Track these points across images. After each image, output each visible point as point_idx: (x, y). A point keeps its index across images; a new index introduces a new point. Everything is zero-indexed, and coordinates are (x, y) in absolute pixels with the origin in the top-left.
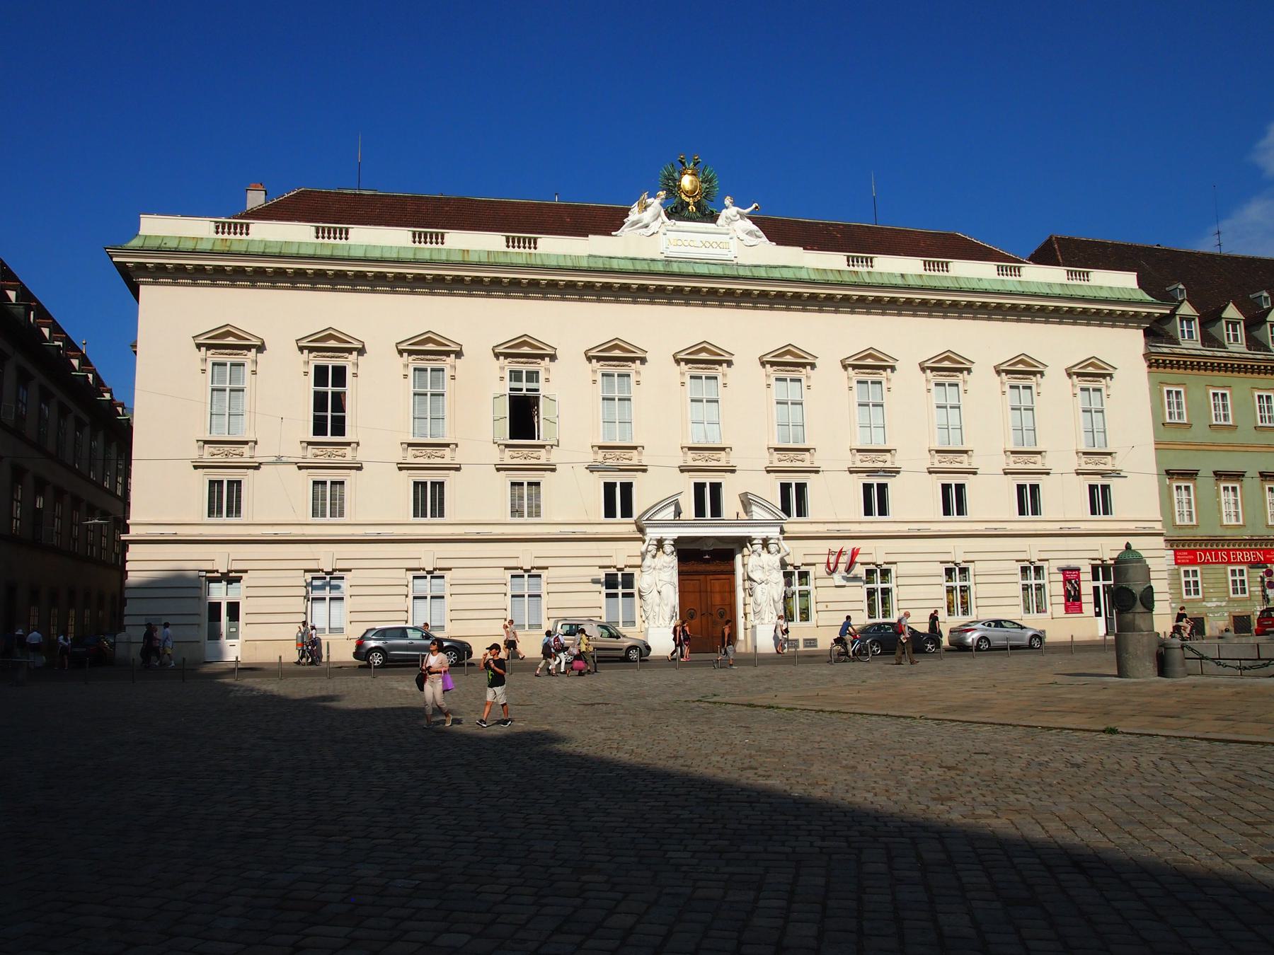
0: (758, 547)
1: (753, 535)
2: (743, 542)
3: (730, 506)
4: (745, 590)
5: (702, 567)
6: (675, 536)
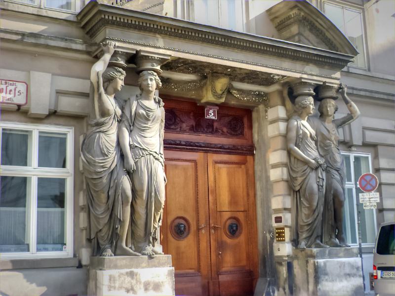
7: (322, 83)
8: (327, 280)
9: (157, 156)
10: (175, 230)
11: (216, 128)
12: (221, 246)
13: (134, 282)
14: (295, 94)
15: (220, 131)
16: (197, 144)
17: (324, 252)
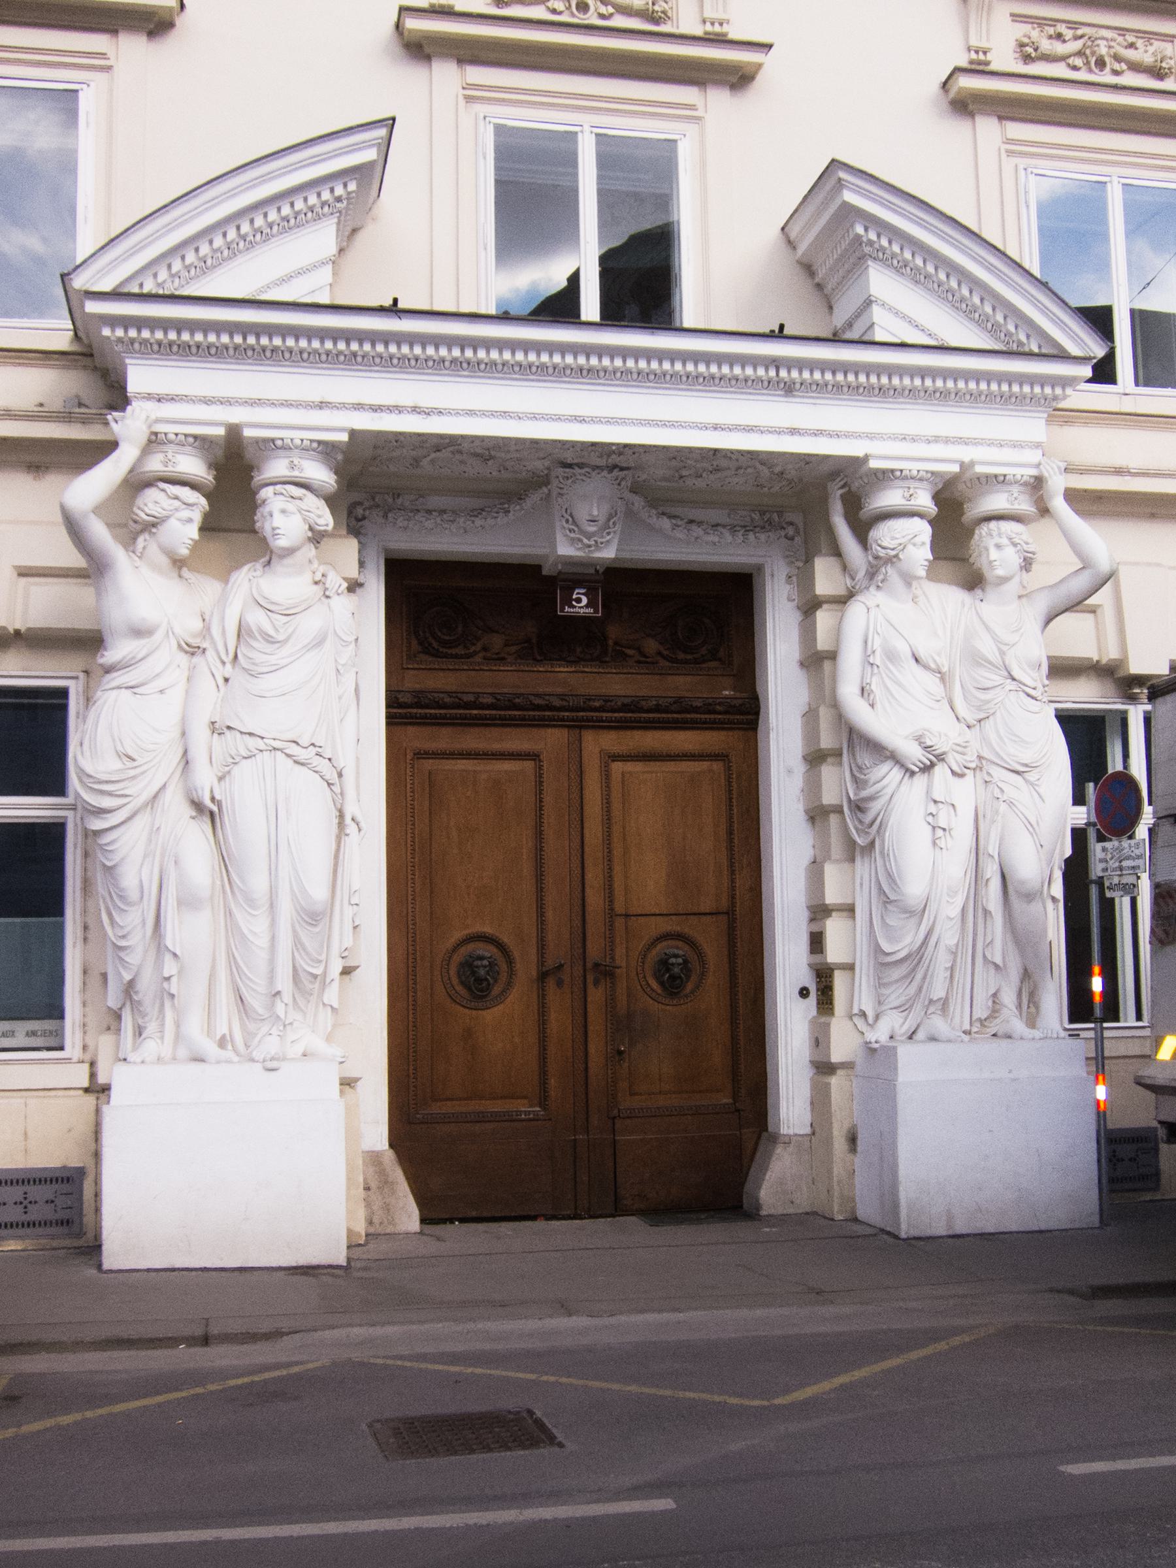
0: (911, 539)
1: (880, 455)
2: (813, 504)
3: (722, 266)
4: (817, 814)
5: (562, 679)
6: (337, 426)
10: (459, 976)
11: (616, 643)
12: (624, 1026)
14: (865, 514)
15: (630, 652)
16: (538, 701)
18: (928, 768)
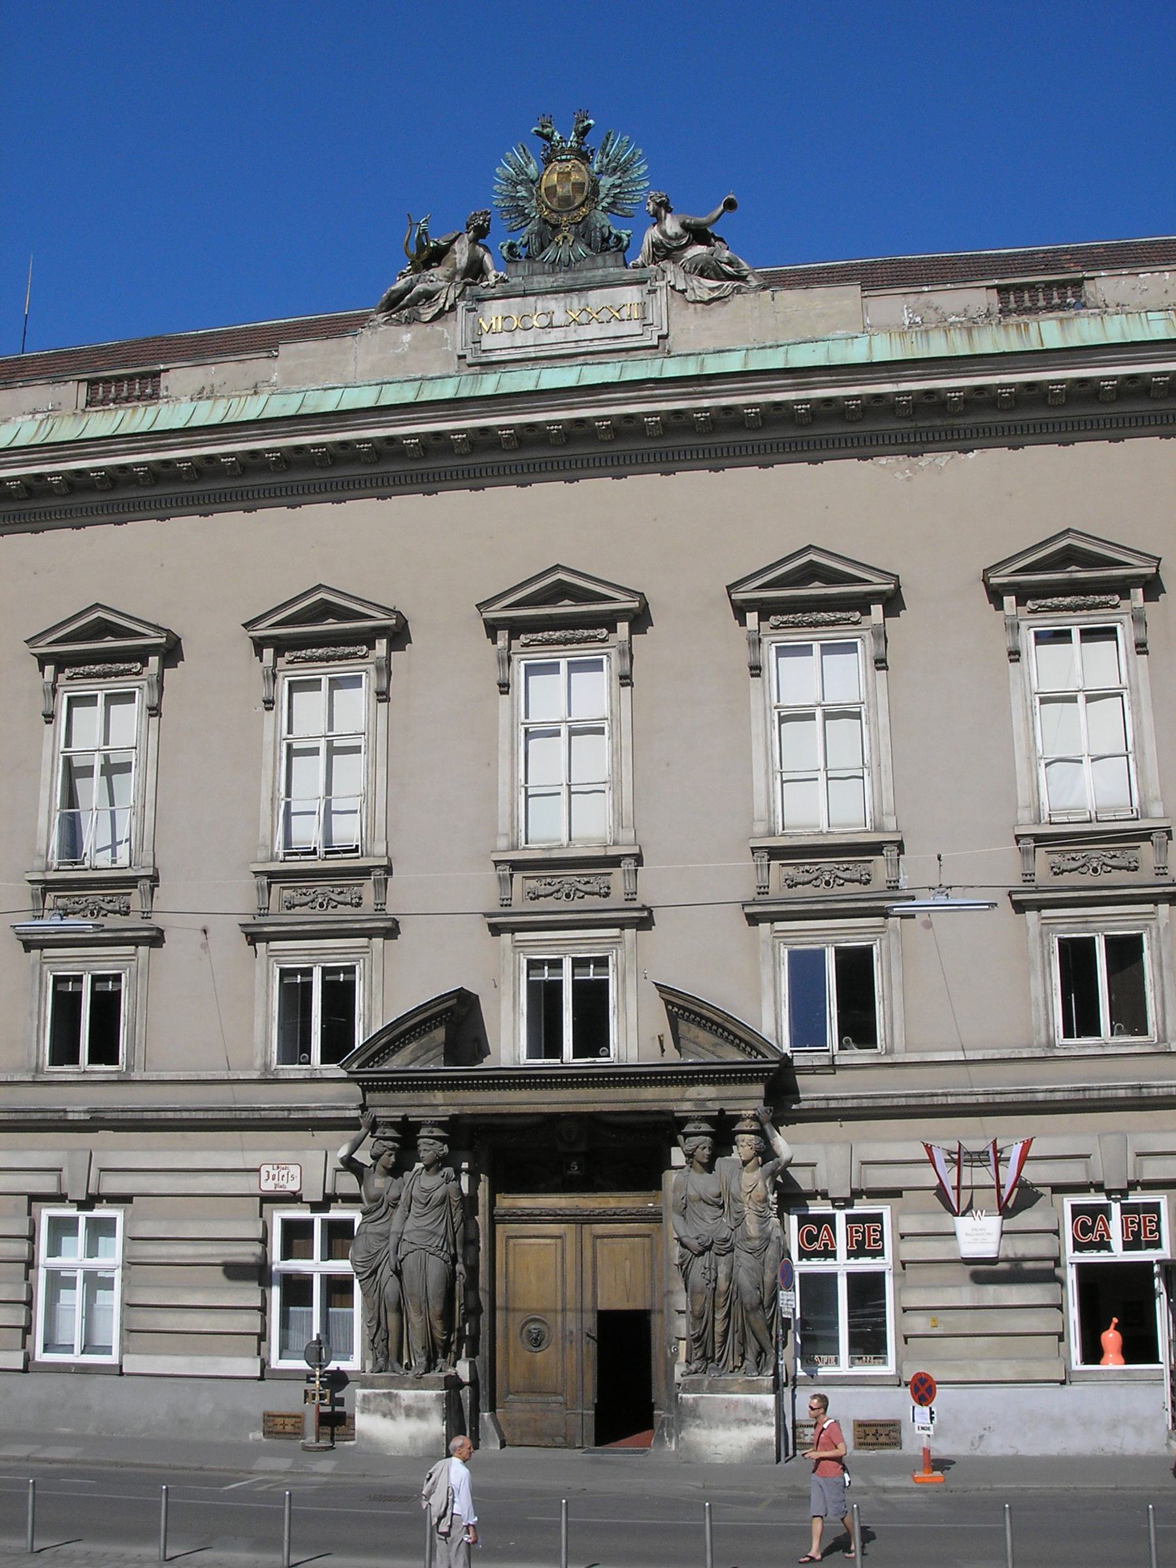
0: (702, 1145)
7: (716, 1113)
8: (697, 1426)
9: (432, 1250)
13: (392, 1405)
17: (700, 1382)
18: (701, 1254)
